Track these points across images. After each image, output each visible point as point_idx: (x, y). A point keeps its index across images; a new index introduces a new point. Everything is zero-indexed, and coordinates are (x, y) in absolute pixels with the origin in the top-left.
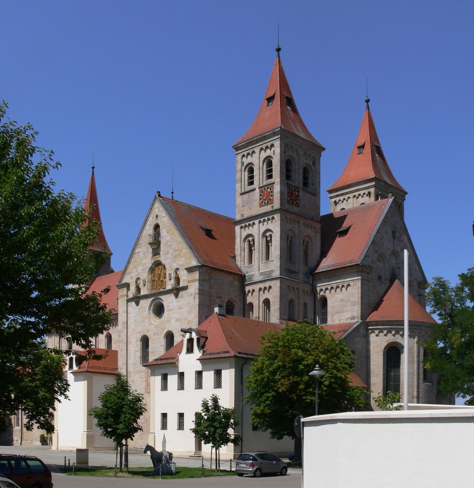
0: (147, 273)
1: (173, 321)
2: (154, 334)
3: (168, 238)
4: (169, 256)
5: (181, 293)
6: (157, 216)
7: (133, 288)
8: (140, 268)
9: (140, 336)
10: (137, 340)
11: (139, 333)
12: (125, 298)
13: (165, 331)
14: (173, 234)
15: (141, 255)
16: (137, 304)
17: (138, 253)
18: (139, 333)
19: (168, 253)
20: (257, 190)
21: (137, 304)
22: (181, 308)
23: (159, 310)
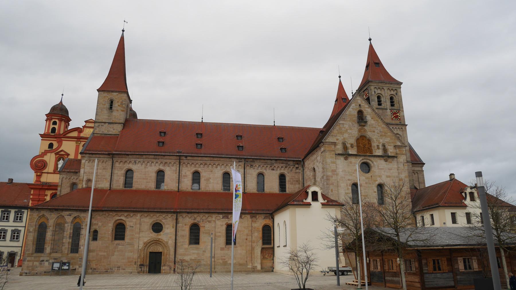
0: (354, 140)
1: (384, 177)
2: (366, 183)
3: (373, 122)
4: (376, 133)
5: (390, 160)
6: (360, 105)
7: (339, 148)
8: (346, 135)
9: (350, 183)
10: (347, 185)
11: (349, 180)
12: (334, 153)
13: (377, 183)
14: (378, 121)
15: (346, 126)
16: (346, 159)
17: (343, 124)
18: (349, 180)
19: (374, 132)
20: (389, 111)
21: (346, 159)
22: (391, 169)
23: (366, 167)
